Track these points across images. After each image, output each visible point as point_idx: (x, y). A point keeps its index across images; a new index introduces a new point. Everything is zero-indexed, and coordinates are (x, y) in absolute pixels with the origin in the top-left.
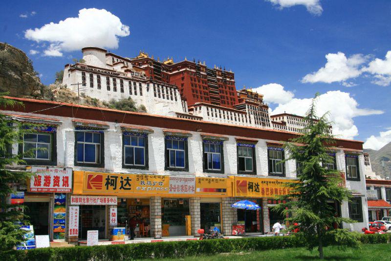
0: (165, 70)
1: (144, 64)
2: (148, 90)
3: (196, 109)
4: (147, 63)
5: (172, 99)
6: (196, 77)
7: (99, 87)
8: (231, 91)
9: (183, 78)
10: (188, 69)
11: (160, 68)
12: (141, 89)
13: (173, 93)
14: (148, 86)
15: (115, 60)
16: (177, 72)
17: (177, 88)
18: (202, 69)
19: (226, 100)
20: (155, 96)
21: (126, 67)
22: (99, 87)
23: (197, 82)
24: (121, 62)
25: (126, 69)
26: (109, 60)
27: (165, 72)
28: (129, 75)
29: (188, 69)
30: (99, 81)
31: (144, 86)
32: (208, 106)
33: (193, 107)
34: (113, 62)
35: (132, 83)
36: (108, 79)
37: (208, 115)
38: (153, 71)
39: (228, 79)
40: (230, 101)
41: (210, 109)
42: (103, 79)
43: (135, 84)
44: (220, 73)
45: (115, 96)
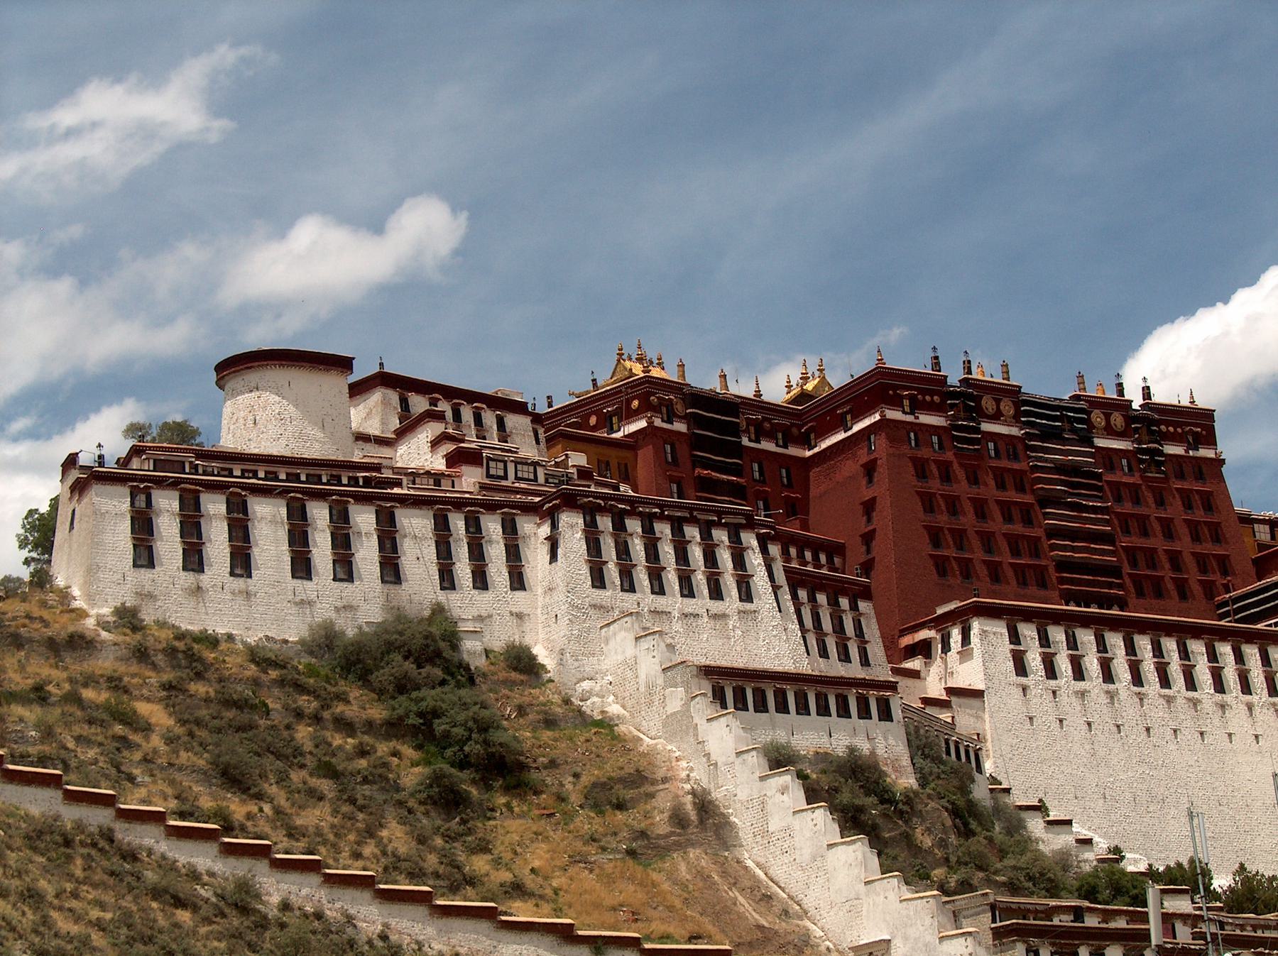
1: (631, 415)
2: (554, 557)
3: (946, 648)
5: (716, 593)
6: (949, 455)
7: (242, 561)
8: (1199, 515)
9: (870, 469)
10: (894, 415)
11: (735, 430)
12: (514, 554)
13: (725, 558)
14: (554, 526)
15: (419, 404)
16: (841, 436)
17: (751, 525)
18: (988, 403)
19: (1166, 572)
20: (599, 581)
22: (242, 561)
23: (961, 487)
24: (440, 417)
25: (449, 447)
29: (894, 415)
31: (534, 532)
32: (1013, 617)
33: (924, 634)
35: (458, 523)
37: (1021, 669)
38: (683, 451)
39: (1173, 449)
40: (1193, 576)
41: (1028, 631)
42: (268, 518)
43: (474, 526)
44: (1118, 420)
45: (348, 608)
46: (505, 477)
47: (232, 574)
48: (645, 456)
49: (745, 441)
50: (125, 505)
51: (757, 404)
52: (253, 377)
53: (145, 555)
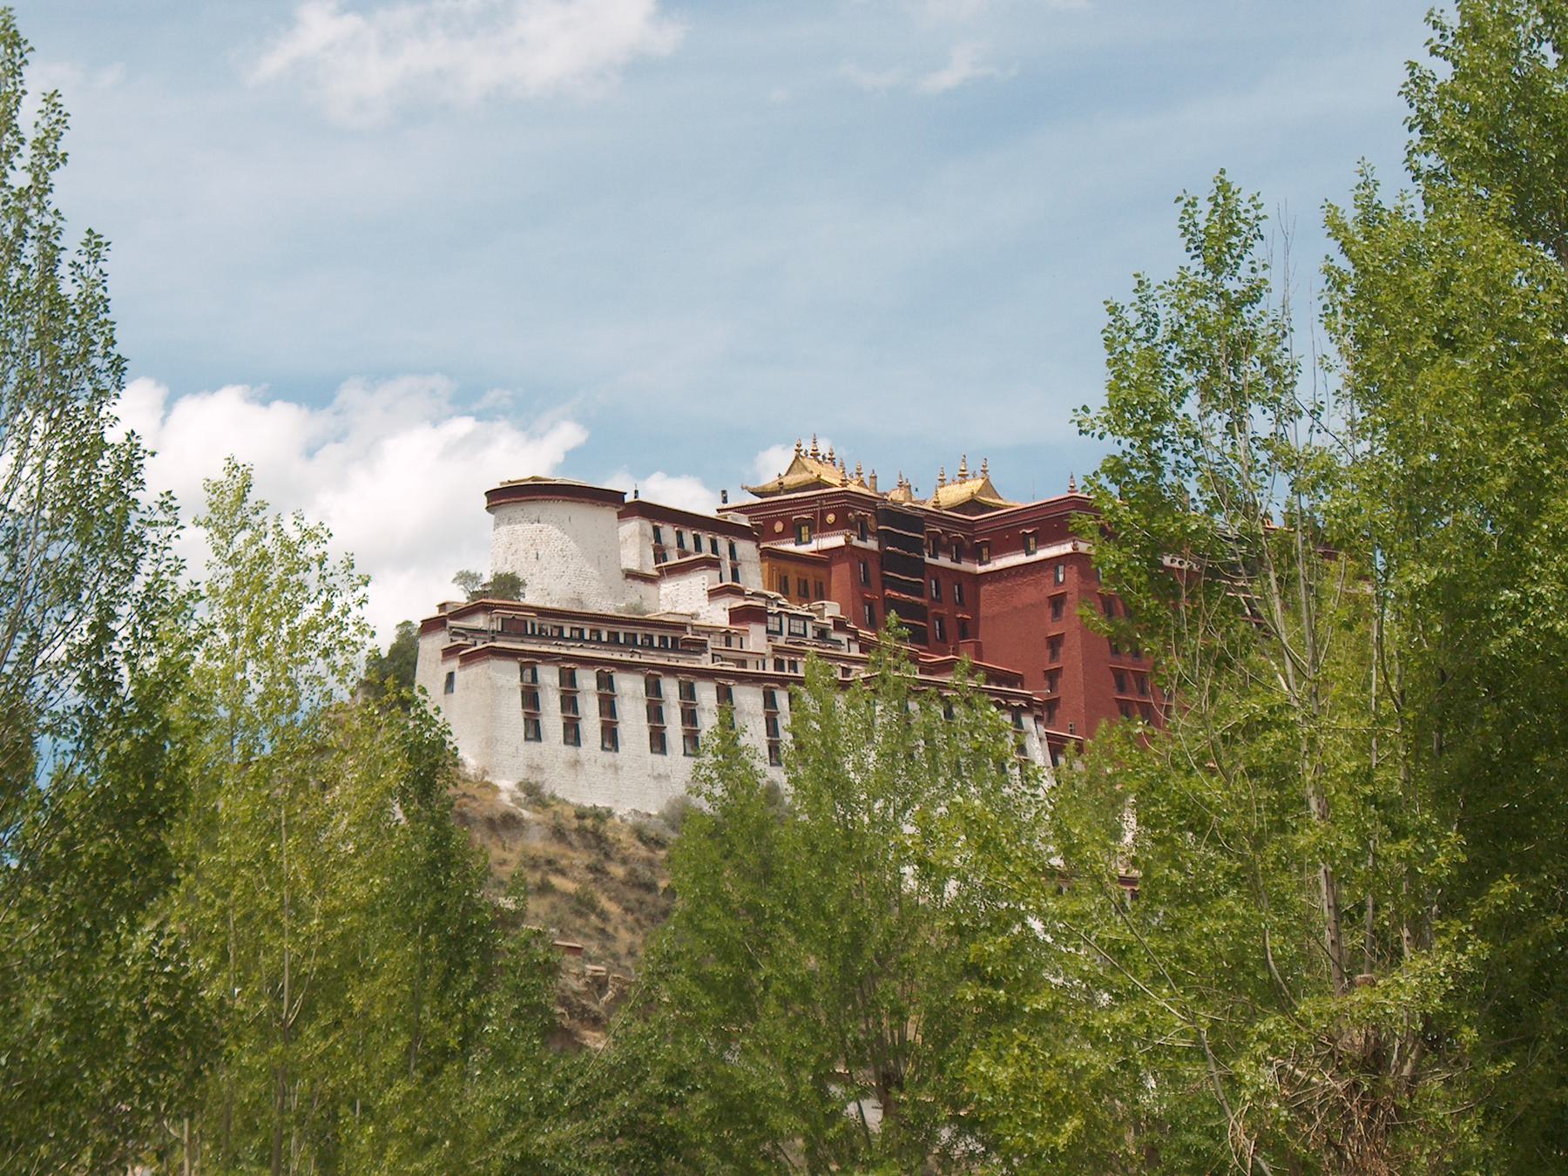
0: (946, 550)
1: (826, 529)
4: (842, 524)
7: (610, 736)
9: (1057, 602)
11: (917, 545)
16: (1020, 559)
21: (739, 592)
22: (610, 736)
24: (713, 564)
26: (632, 544)
27: (944, 561)
28: (755, 639)
30: (608, 706)
34: (660, 554)
36: (653, 689)
38: (874, 568)
46: (780, 633)
47: (603, 748)
48: (841, 575)
49: (928, 560)
50: (516, 681)
51: (935, 517)
52: (534, 509)
53: (534, 730)
